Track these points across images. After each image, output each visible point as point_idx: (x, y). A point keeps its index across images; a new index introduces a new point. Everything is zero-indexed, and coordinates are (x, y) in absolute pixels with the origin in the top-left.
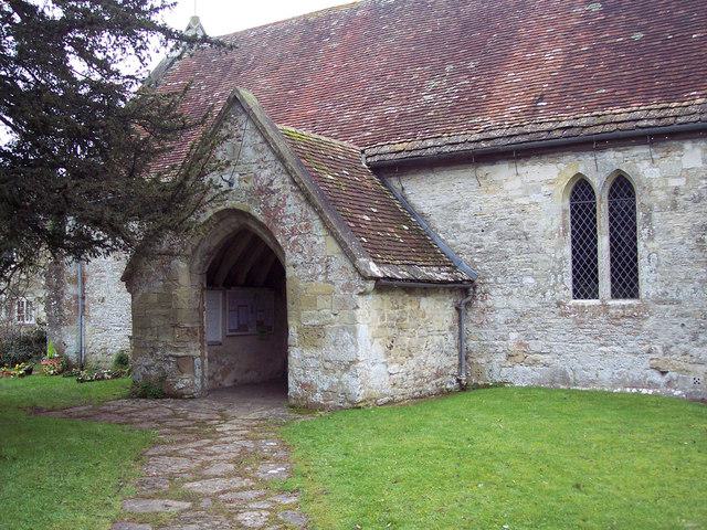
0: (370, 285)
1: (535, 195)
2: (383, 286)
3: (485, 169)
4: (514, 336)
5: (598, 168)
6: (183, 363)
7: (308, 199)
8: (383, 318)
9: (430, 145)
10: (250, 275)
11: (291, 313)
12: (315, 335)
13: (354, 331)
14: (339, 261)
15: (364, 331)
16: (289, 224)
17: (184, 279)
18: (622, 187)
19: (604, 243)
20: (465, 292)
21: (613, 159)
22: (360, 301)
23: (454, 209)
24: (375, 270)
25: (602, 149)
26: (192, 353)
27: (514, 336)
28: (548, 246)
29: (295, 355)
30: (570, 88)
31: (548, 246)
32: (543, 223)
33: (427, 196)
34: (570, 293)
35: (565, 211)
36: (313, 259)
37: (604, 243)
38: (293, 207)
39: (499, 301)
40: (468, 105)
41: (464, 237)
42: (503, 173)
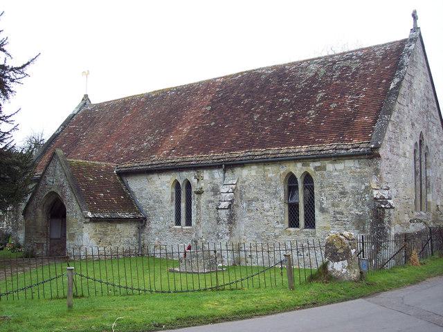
0: (88, 220)
1: (163, 185)
2: (94, 220)
3: (151, 176)
4: (157, 239)
5: (298, 170)
6: (40, 245)
7: (72, 190)
8: (96, 231)
9: (135, 165)
10: (57, 211)
11: (67, 229)
12: (72, 236)
13: (82, 235)
14: (79, 212)
15: (86, 235)
16: (67, 198)
17: (40, 215)
18: (308, 178)
19: (183, 205)
20: (142, 222)
21: (185, 175)
22: (85, 225)
23: (141, 190)
24: (89, 214)
25: (182, 171)
26: (43, 242)
27: (157, 239)
28: (167, 205)
29: (68, 243)
30: (182, 148)
31: (167, 205)
32: (166, 196)
33: (135, 184)
34: (174, 223)
35: (172, 193)
36: (73, 208)
37: (183, 205)
38: (69, 192)
39: (154, 225)
40: (154, 149)
41: (144, 201)
42: (155, 177)
